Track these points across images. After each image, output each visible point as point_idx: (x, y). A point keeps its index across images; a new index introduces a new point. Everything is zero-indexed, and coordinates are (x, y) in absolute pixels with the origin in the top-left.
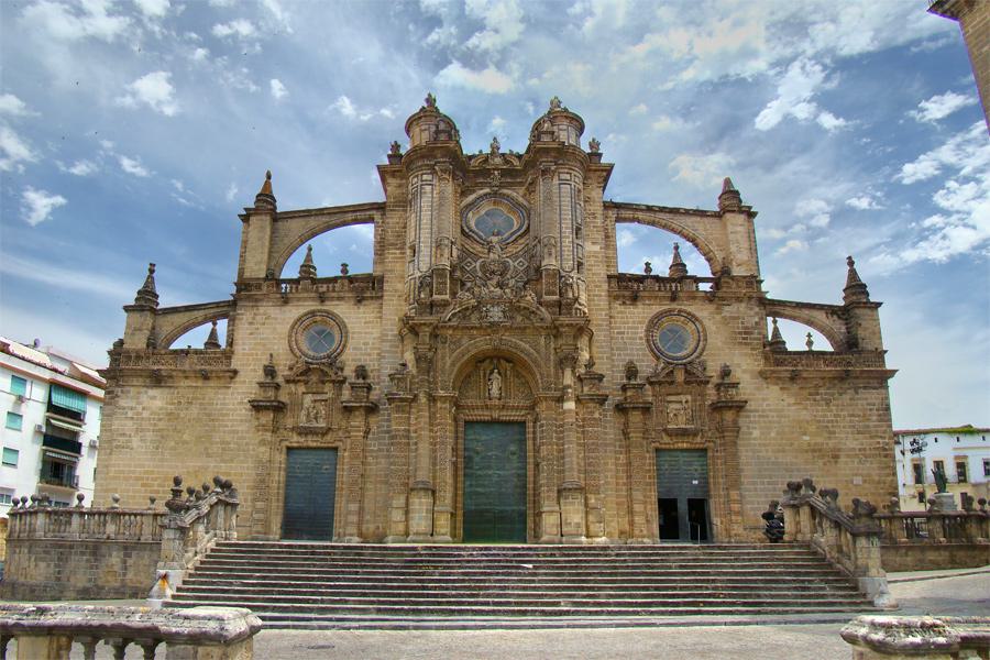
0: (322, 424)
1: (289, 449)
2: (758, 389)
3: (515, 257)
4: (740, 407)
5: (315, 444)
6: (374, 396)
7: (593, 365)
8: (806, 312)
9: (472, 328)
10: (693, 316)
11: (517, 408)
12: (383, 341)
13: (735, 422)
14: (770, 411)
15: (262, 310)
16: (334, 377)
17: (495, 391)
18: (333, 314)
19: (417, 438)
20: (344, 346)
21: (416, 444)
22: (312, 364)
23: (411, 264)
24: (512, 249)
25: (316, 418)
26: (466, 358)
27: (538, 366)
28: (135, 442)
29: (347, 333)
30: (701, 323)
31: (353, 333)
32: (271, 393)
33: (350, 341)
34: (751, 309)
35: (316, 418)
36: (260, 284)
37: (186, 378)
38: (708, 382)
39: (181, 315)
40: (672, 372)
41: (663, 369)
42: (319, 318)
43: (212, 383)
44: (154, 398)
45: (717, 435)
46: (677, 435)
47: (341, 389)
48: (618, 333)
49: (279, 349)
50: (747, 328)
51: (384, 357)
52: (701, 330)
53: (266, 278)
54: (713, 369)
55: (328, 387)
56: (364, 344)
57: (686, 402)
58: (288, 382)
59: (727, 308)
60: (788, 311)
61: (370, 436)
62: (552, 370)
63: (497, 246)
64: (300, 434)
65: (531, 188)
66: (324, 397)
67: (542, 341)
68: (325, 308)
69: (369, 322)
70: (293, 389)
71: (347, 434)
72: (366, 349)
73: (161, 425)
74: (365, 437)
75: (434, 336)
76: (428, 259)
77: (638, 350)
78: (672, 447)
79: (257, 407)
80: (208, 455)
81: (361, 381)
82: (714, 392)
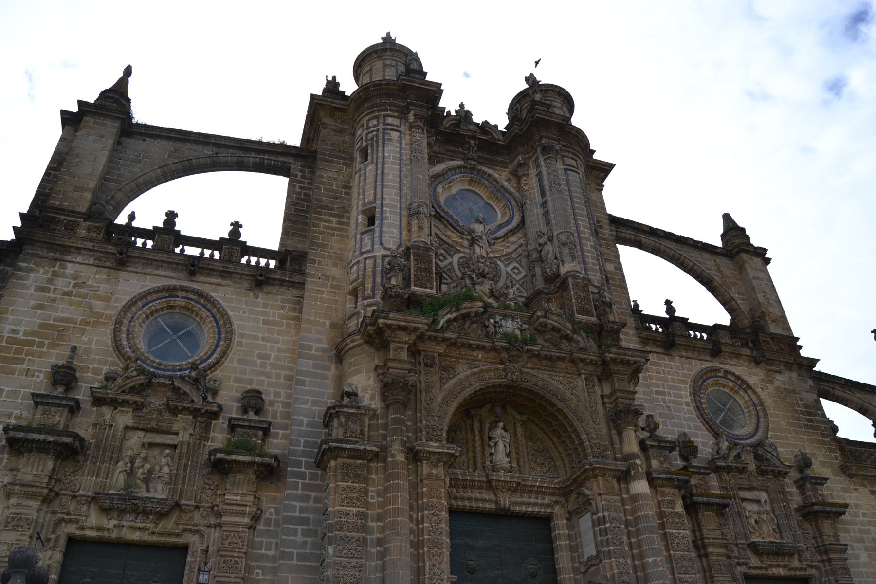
0: (159, 492)
1: (72, 541)
2: (845, 490)
3: (507, 259)
4: (837, 512)
5: (136, 536)
6: (276, 445)
7: (656, 426)
8: (858, 396)
9: (478, 347)
10: (744, 382)
11: (539, 492)
12: (301, 356)
13: (837, 537)
14: (869, 523)
15: (70, 269)
16: (198, 403)
17: (501, 457)
18: (208, 298)
19: (382, 530)
20: (224, 354)
21: (379, 542)
22: (154, 375)
23: (367, 238)
24: (501, 248)
25: (146, 481)
26: (466, 393)
27: (580, 420)
29: (230, 332)
30: (755, 393)
31: (242, 336)
32: (59, 418)
33: (234, 347)
34: (805, 382)
35: (146, 481)
36: (78, 224)
40: (739, 454)
41: (730, 449)
42: (180, 302)
45: (819, 558)
46: (768, 554)
47: (207, 428)
48: (657, 393)
49: (90, 342)
50: (806, 406)
51: (303, 383)
52: (756, 402)
53: (88, 216)
56: (260, 356)
57: (765, 501)
58: (98, 401)
59: (778, 377)
61: (261, 527)
62: (604, 430)
63: (484, 237)
64: (106, 511)
65: (516, 175)
66: (169, 439)
67: (581, 382)
68: (195, 286)
69: (274, 323)
70: (108, 417)
71: (212, 521)
72: (263, 365)
74: (252, 528)
75: (414, 352)
76: (396, 231)
77: (686, 419)
78: (764, 572)
81: (251, 415)
82: (794, 490)
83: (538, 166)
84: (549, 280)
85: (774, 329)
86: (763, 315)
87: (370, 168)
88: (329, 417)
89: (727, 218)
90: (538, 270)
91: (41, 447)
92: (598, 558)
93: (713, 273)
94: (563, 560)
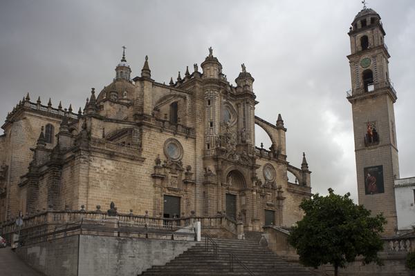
4: (283, 199)
8: (295, 171)
15: (153, 133)
28: (101, 184)
37: (124, 158)
38: (275, 190)
39: (113, 124)
43: (135, 162)
44: (109, 164)
54: (277, 185)
55: (178, 172)
60: (292, 170)
64: (169, 190)
73: (113, 178)
79: (154, 177)
80: (135, 195)
83: (244, 106)
84: (242, 142)
85: (283, 153)
86: (281, 149)
87: (211, 108)
88: (206, 176)
89: (280, 115)
90: (240, 138)
91: (159, 177)
92: (246, 205)
93: (273, 134)
94: (238, 204)
